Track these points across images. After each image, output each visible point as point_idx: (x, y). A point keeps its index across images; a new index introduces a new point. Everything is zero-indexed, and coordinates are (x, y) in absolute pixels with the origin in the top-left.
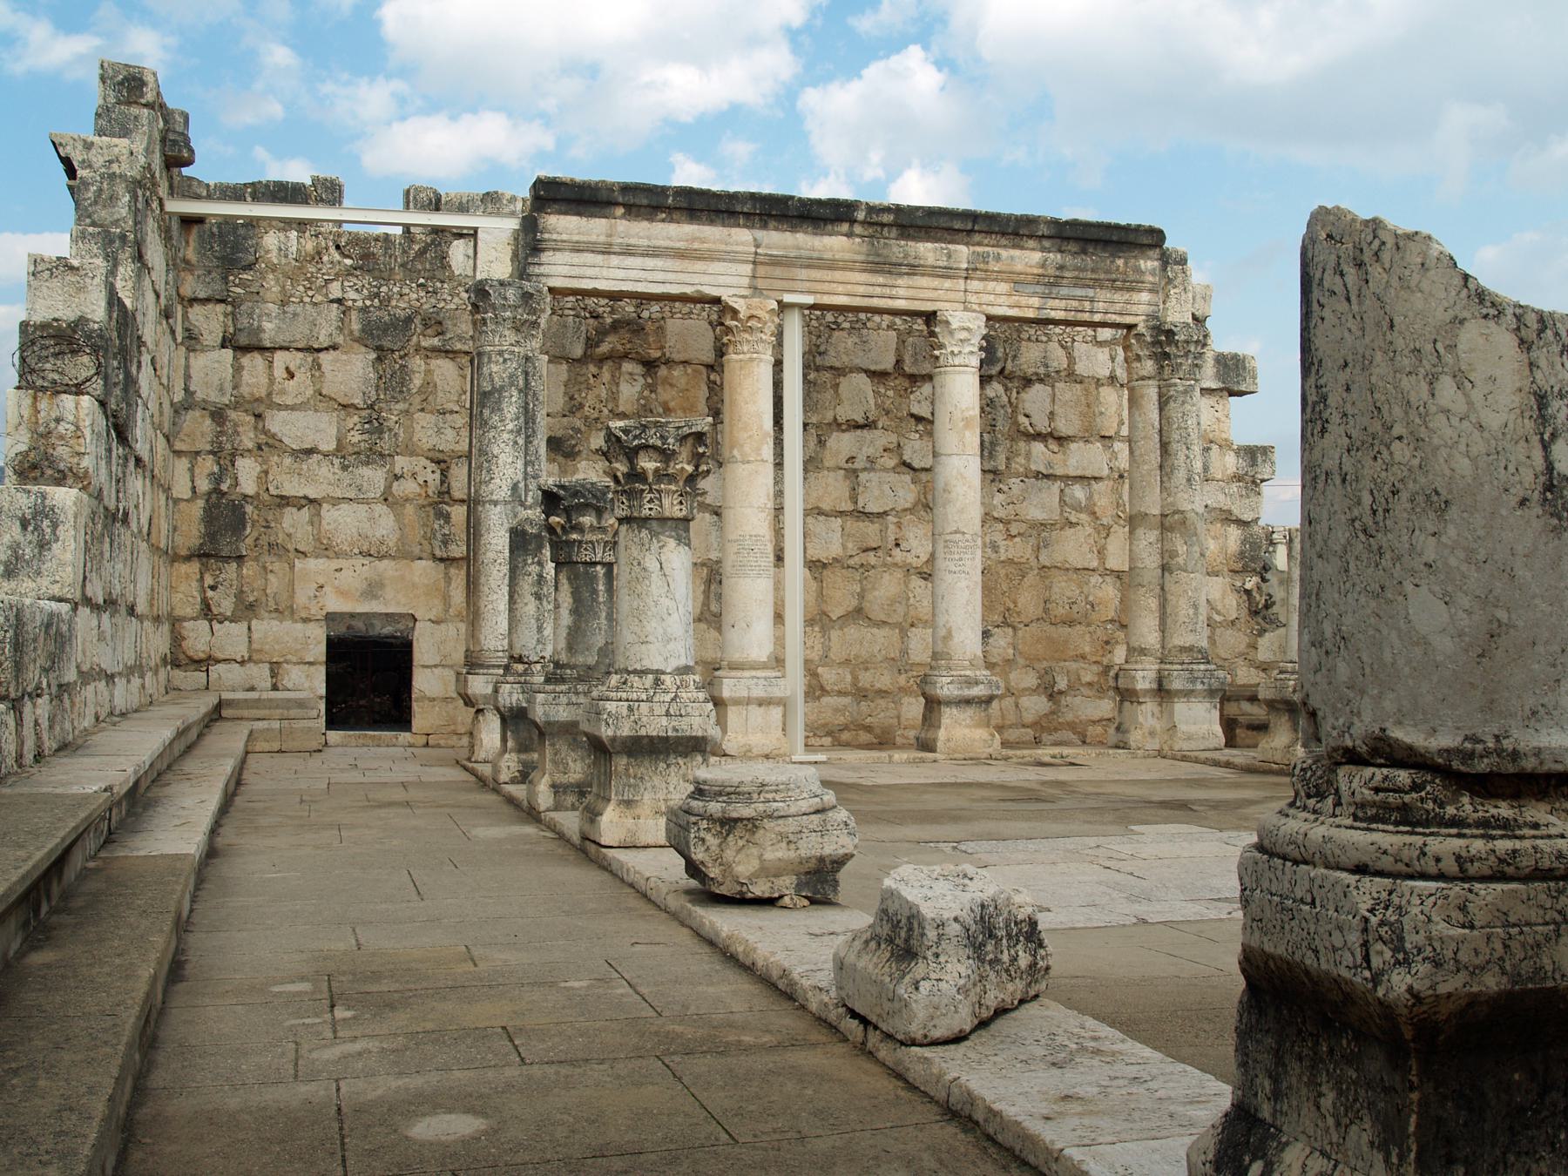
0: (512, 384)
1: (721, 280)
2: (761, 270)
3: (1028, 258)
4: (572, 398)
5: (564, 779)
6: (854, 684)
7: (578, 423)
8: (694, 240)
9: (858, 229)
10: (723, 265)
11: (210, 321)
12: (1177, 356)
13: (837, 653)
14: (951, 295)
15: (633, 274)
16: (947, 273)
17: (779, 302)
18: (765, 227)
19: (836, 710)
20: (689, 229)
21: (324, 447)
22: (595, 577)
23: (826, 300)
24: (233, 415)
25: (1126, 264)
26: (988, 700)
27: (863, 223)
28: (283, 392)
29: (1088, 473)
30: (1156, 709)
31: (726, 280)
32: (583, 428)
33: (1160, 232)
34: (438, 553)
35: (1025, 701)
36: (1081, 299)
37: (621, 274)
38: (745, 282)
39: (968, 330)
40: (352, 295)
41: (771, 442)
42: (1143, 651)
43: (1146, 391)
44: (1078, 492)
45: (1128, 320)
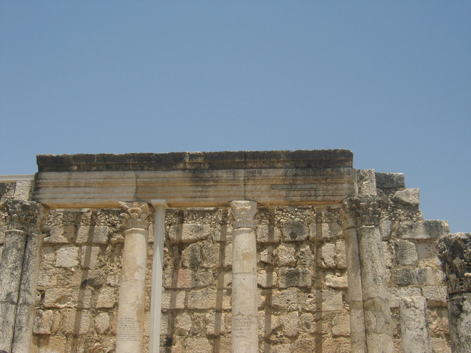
0: (13, 247)
7: (102, 272)
18: (142, 169)
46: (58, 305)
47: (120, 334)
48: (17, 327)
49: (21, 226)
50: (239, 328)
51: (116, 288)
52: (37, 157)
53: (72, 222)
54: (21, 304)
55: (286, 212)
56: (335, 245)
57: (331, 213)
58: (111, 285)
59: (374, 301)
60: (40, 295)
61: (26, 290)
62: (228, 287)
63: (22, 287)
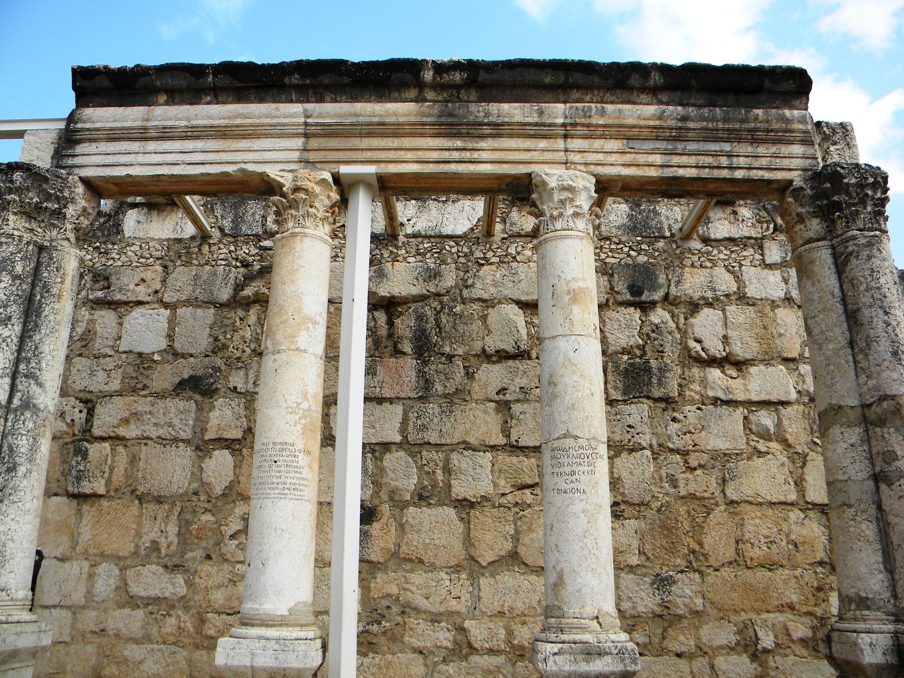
1: (267, 156)
2: (314, 143)
3: (642, 112)
4: (216, 339)
6: (509, 642)
7: (219, 362)
8: (238, 116)
9: (430, 95)
10: (270, 143)
12: (849, 205)
14: (548, 156)
17: (337, 178)
18: (321, 100)
25: (766, 114)
27: (437, 87)
29: (773, 397)
31: (275, 159)
32: (223, 367)
34: (70, 489)
35: (721, 662)
36: (715, 154)
38: (296, 155)
39: (570, 189)
43: (816, 254)
44: (766, 419)
46: (122, 431)
47: (261, 484)
49: (27, 225)
50: (567, 469)
51: (249, 398)
52: (74, 71)
53: (158, 259)
54: (16, 410)
55: (617, 244)
56: (724, 314)
57: (711, 249)
58: (238, 390)
59: (898, 403)
60: (85, 411)
62: (497, 398)
63: (22, 367)
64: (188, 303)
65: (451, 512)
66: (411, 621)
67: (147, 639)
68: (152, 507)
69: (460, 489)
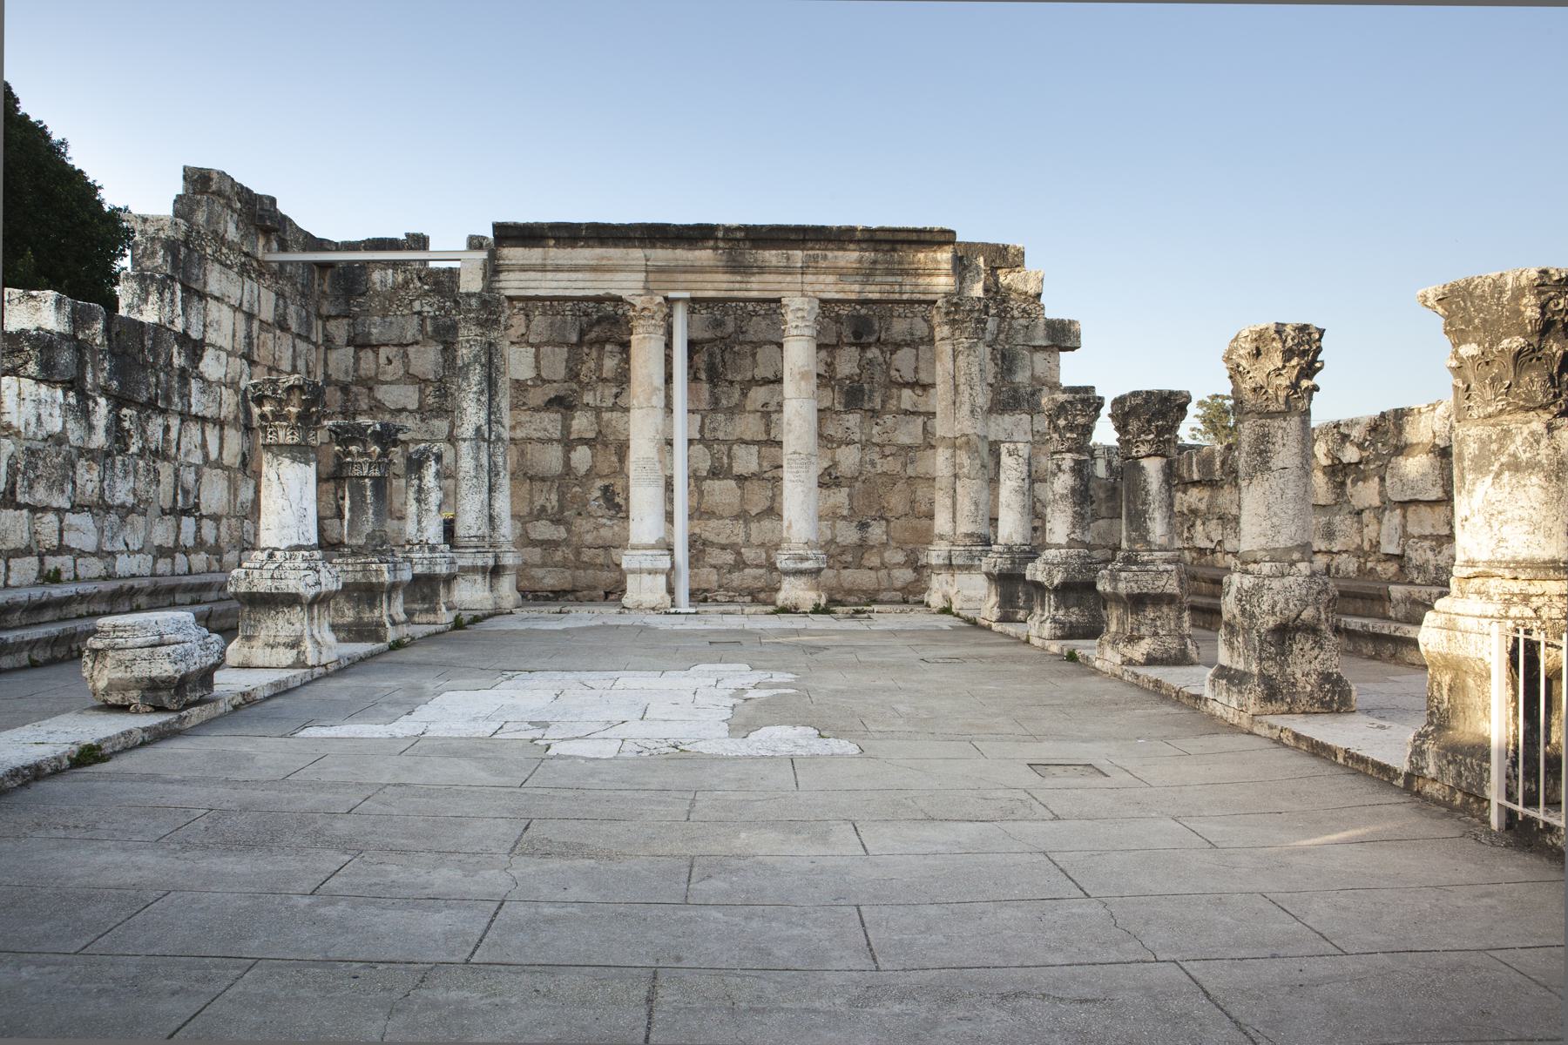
1: (625, 285)
2: (652, 277)
3: (849, 257)
5: (340, 621)
7: (575, 386)
9: (721, 244)
11: (339, 330)
13: (755, 539)
14: (792, 286)
15: (562, 284)
16: (788, 270)
17: (666, 299)
18: (654, 247)
19: (755, 578)
20: (599, 251)
21: (410, 407)
22: (364, 486)
23: (699, 294)
24: (354, 389)
26: (819, 570)
27: (723, 239)
28: (384, 373)
30: (950, 579)
31: (627, 285)
33: (953, 233)
37: (554, 284)
40: (427, 308)
41: (662, 394)
42: (941, 537)
45: (930, 297)
48: (493, 472)
61: (498, 422)
64: (547, 343)
65: (733, 483)
66: (708, 550)
67: (544, 565)
68: (537, 485)
69: (738, 468)
